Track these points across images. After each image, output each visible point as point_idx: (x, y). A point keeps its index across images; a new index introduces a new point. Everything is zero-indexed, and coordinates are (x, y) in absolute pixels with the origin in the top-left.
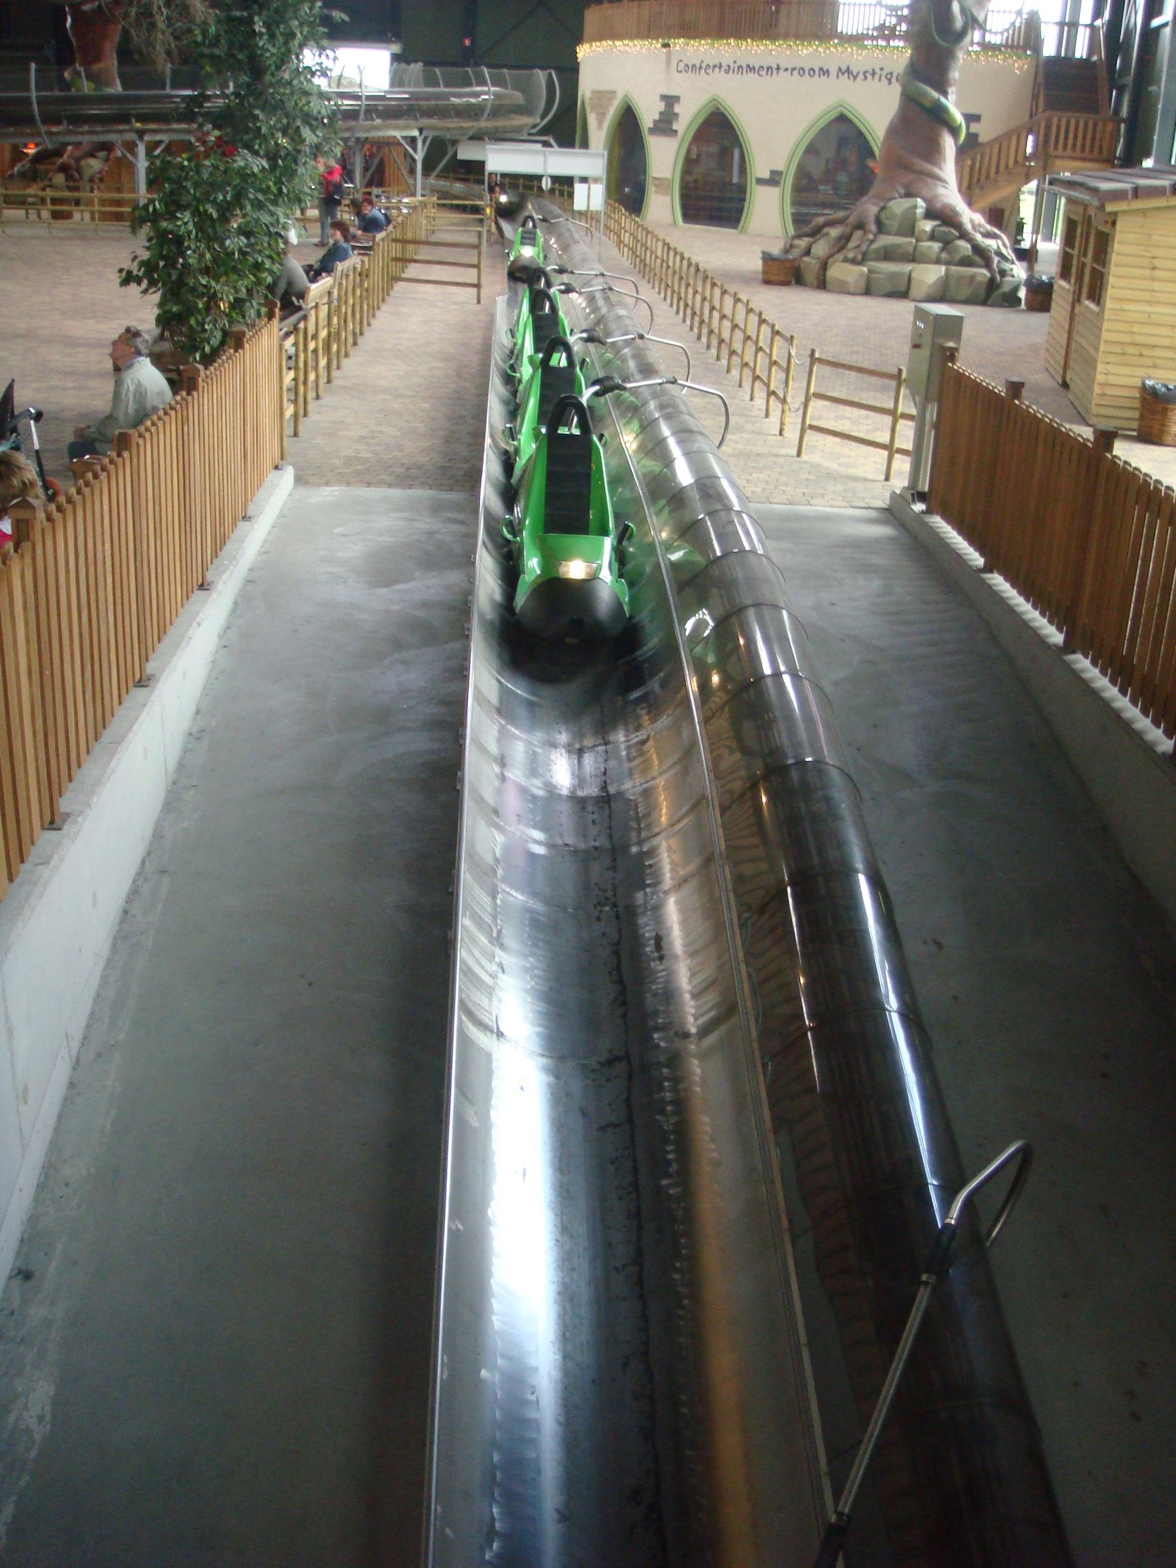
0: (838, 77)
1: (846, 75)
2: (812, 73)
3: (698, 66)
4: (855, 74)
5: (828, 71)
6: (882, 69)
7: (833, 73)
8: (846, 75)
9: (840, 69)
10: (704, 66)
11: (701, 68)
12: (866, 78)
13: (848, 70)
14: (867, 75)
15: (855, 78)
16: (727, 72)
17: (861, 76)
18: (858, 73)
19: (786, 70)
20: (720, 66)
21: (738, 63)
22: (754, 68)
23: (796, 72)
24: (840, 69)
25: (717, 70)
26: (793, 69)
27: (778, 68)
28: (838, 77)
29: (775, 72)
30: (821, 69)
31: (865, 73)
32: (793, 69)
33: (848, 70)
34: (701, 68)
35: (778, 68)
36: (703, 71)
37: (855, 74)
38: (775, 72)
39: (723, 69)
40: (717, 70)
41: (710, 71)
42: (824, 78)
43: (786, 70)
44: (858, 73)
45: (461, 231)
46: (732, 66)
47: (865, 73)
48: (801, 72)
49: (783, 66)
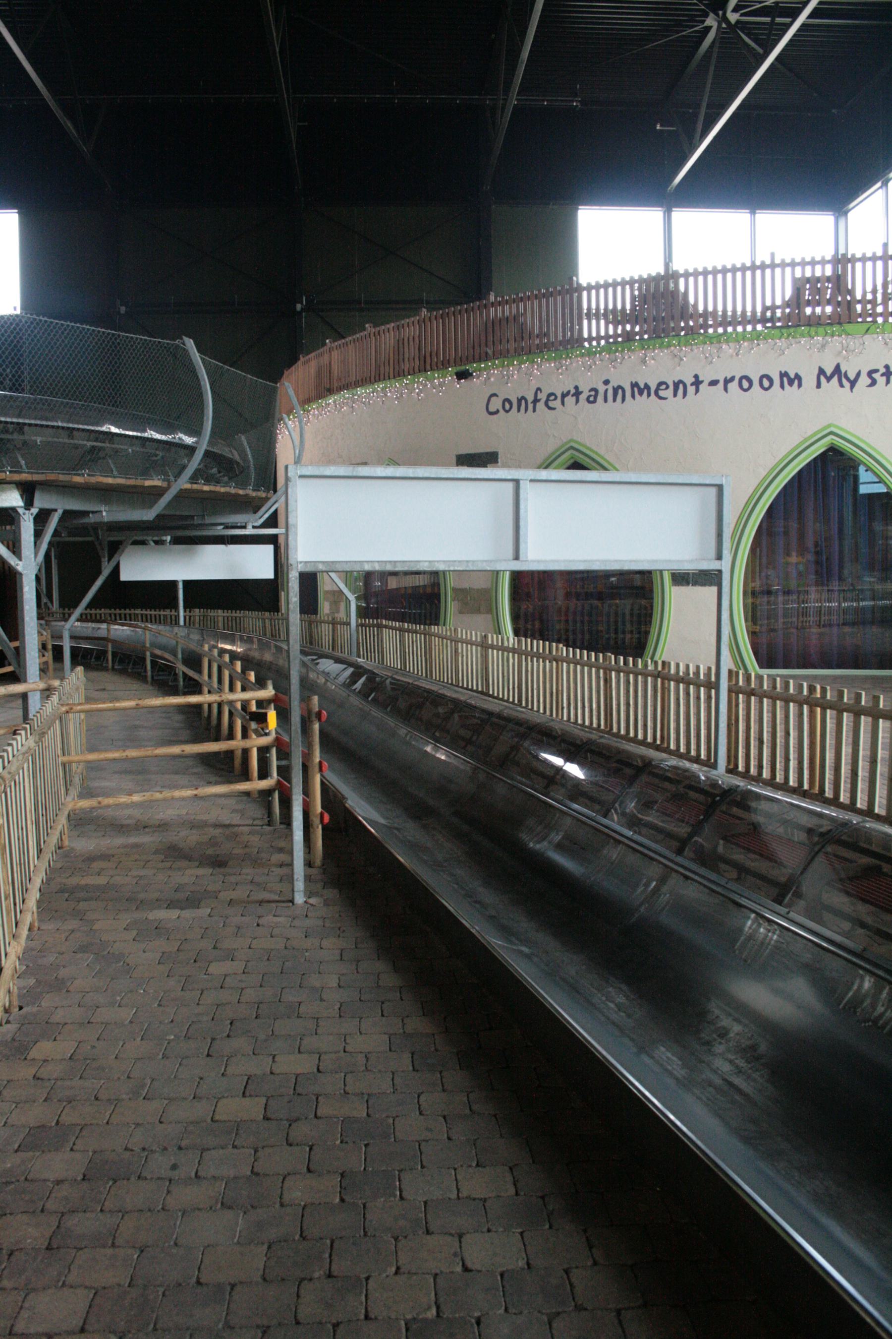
0: (819, 386)
1: (835, 379)
2: (766, 383)
3: (530, 398)
4: (852, 376)
5: (798, 377)
6: (606, 382)
7: (809, 380)
8: (835, 379)
9: (821, 372)
10: (542, 396)
11: (536, 401)
12: (874, 383)
13: (837, 369)
14: (876, 376)
15: (853, 384)
16: (591, 400)
17: (864, 380)
18: (859, 374)
19: (714, 383)
20: (577, 393)
21: (614, 383)
22: (647, 387)
23: (733, 386)
24: (821, 372)
25: (570, 400)
26: (727, 381)
27: (697, 383)
28: (819, 386)
29: (691, 389)
30: (634, 385)
31: (870, 373)
32: (727, 381)
33: (837, 369)
34: (536, 401)
35: (697, 383)
36: (541, 406)
37: (852, 376)
38: (691, 389)
39: (583, 397)
40: (570, 400)
41: (556, 404)
42: (791, 391)
43: (714, 383)
44: (859, 374)
45: (868, 1270)
46: (601, 389)
47: (870, 373)
48: (745, 384)
49: (706, 377)
